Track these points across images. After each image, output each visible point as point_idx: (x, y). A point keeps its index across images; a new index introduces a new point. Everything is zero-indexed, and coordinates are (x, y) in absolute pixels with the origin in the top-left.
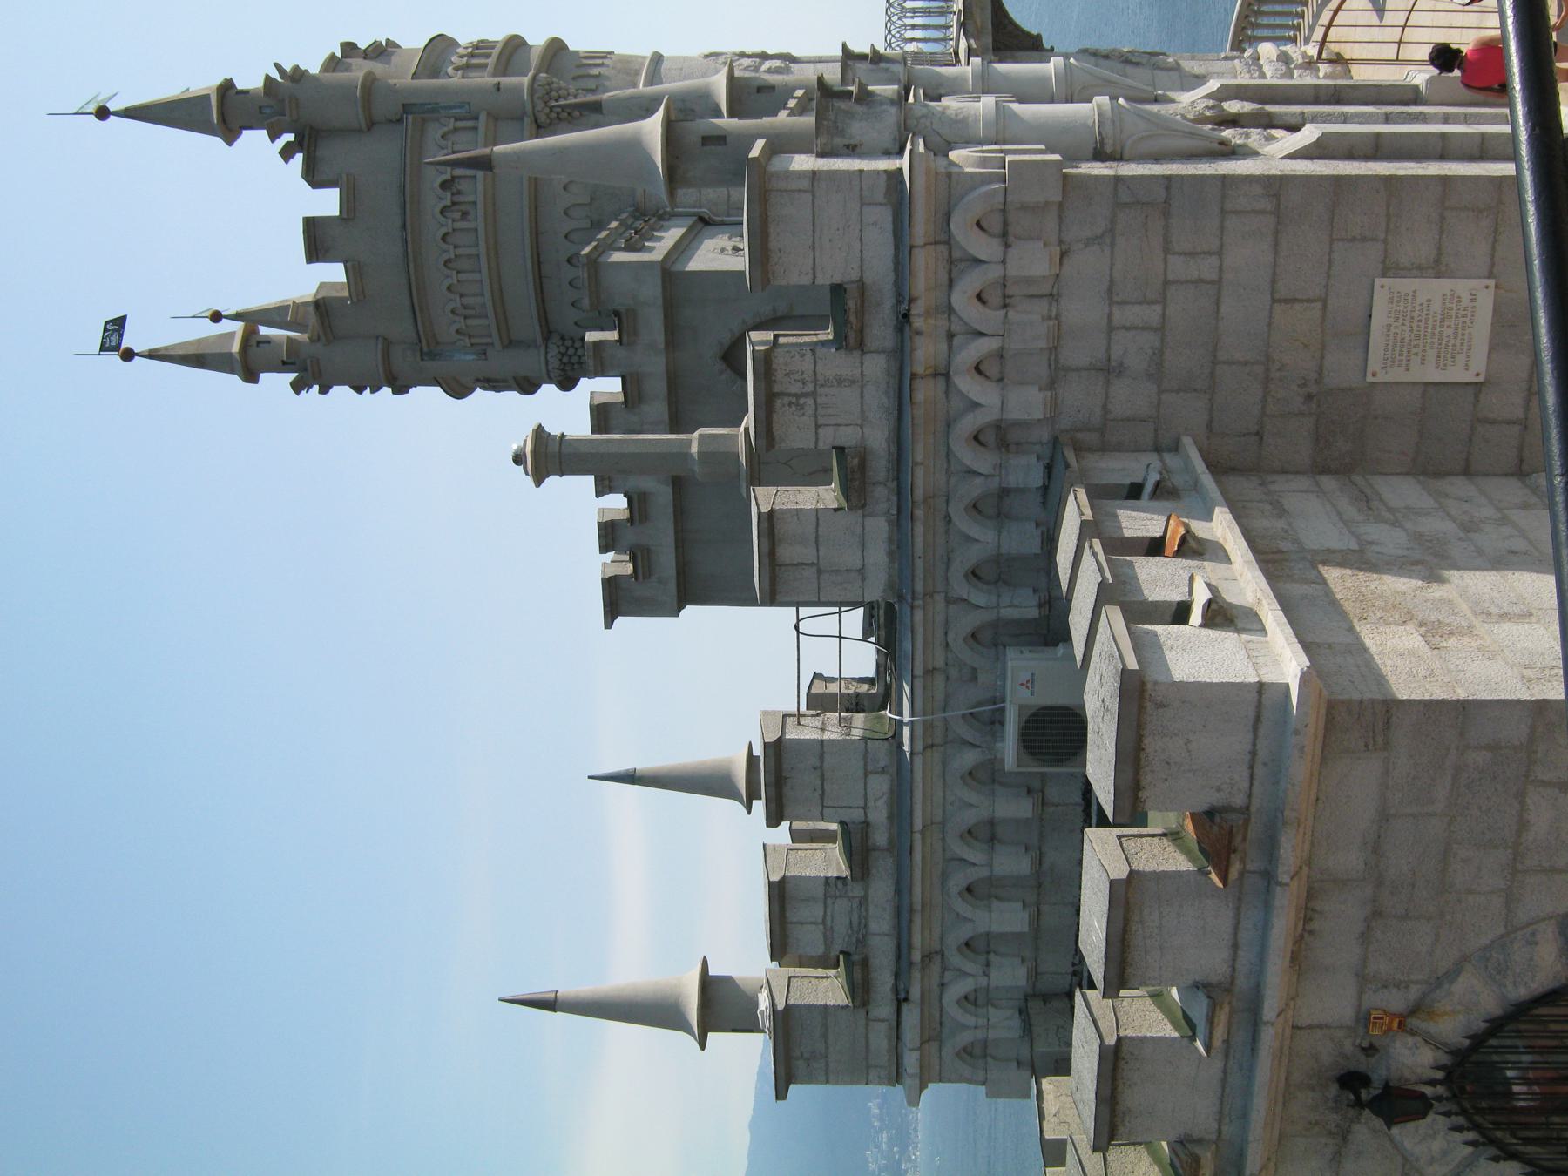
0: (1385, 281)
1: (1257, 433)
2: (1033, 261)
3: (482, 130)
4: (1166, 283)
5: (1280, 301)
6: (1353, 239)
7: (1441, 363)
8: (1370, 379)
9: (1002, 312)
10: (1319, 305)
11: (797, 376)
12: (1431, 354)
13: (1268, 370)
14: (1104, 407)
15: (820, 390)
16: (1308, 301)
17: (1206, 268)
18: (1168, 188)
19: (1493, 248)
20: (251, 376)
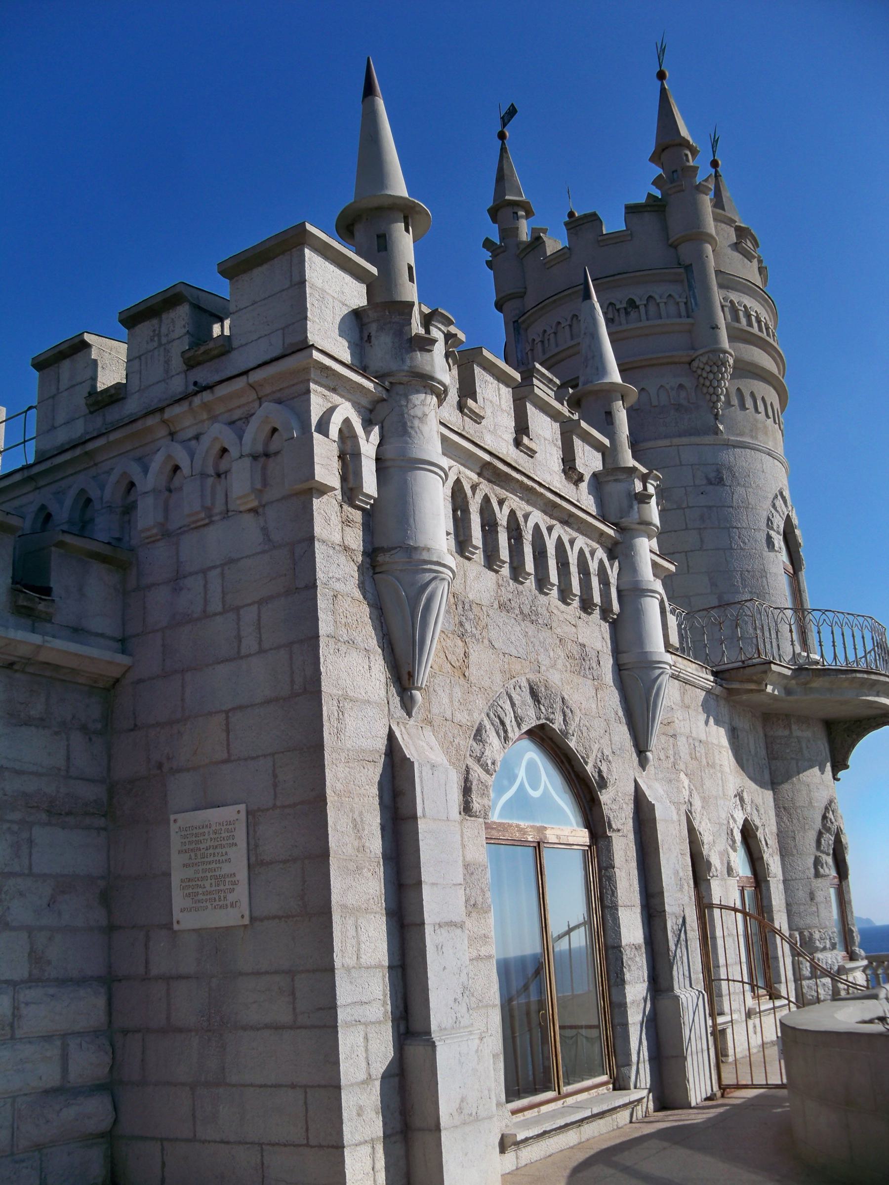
1: (136, 725)
2: (241, 481)
3: (678, 320)
4: (237, 609)
5: (227, 718)
6: (275, 776)
8: (172, 817)
9: (211, 471)
10: (225, 756)
11: (172, 328)
12: (190, 873)
14: (153, 585)
15: (162, 349)
16: (228, 745)
17: (250, 643)
18: (307, 587)
19: (274, 917)
20: (494, 213)
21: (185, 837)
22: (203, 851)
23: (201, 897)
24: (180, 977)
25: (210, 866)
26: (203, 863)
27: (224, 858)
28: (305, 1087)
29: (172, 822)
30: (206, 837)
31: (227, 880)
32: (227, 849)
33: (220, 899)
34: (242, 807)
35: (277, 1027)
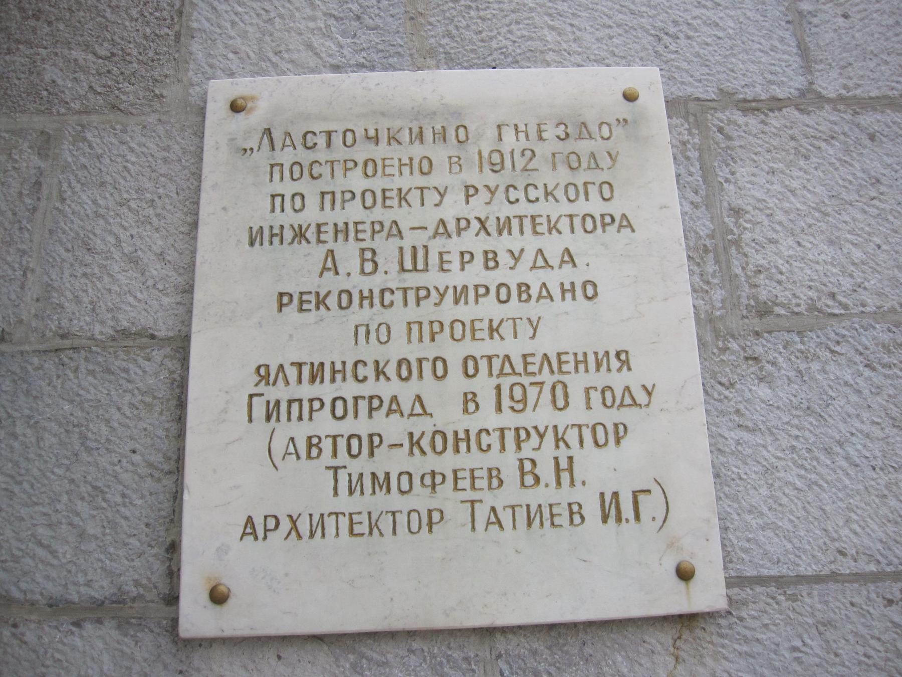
8: (221, 91)
12: (327, 337)
22: (410, 239)
23: (392, 462)
25: (465, 312)
26: (421, 295)
27: (554, 279)
29: (216, 109)
30: (437, 179)
31: (577, 384)
32: (579, 243)
33: (528, 473)
34: (648, 80)
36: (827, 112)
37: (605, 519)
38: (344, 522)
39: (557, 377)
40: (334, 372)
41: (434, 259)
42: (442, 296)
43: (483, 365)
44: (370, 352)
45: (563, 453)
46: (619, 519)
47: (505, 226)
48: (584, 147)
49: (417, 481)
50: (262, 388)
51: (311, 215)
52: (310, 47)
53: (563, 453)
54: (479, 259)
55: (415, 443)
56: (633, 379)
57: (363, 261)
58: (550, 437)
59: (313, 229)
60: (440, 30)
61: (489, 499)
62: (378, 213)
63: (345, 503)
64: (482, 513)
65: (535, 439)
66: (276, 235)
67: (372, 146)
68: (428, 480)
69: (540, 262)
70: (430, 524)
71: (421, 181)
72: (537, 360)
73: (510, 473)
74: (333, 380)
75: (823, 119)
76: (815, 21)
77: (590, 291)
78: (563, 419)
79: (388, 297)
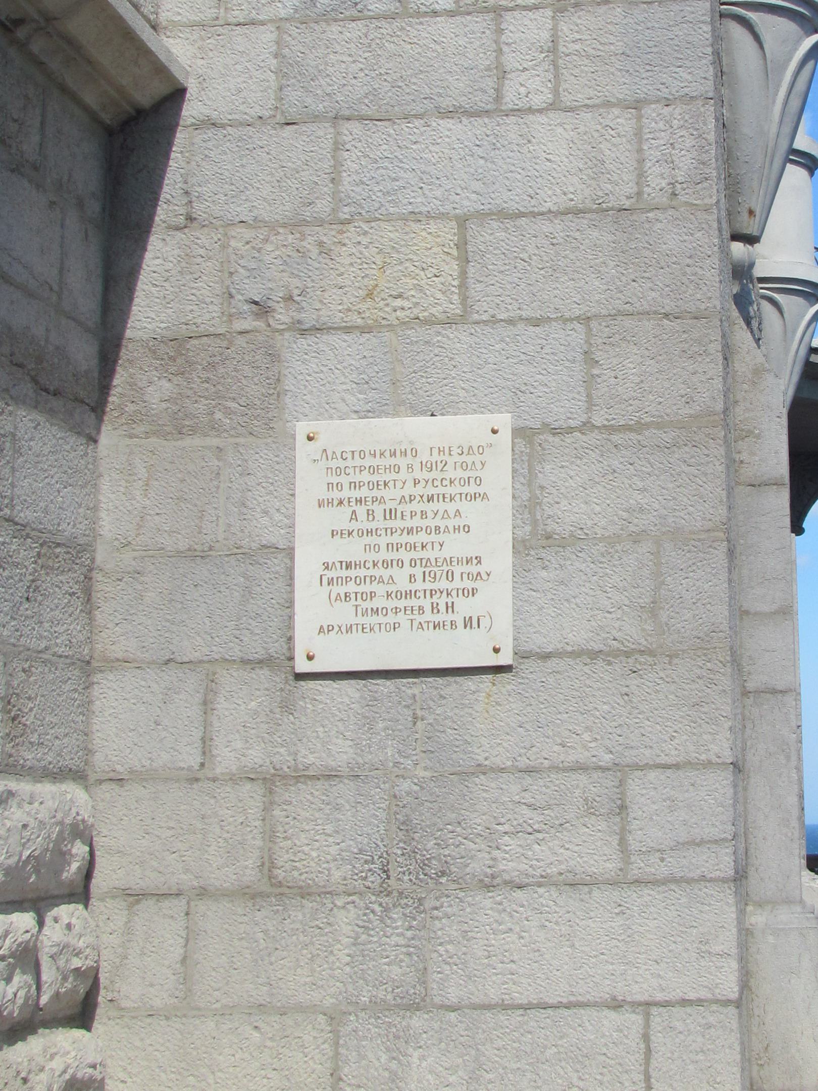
0: (506, 435)
4: (498, 11)
7: (333, 574)
8: (302, 428)
13: (321, 223)
16: (463, 286)
17: (529, 85)
21: (339, 471)
24: (301, 776)
25: (412, 539)
28: (647, 1006)
29: (301, 438)
30: (403, 475)
31: (458, 570)
32: (464, 506)
33: (435, 608)
34: (504, 421)
35: (575, 883)
36: (595, 434)
37: (465, 627)
38: (360, 627)
39: (450, 567)
40: (356, 565)
41: (399, 515)
42: (403, 531)
43: (418, 562)
44: (371, 556)
45: (450, 600)
46: (471, 627)
47: (430, 499)
48: (469, 459)
49: (389, 611)
50: (326, 572)
51: (346, 493)
52: (343, 400)
53: (450, 600)
54: (419, 514)
55: (389, 595)
56: (482, 569)
57: (368, 514)
58: (445, 593)
59: (346, 500)
60: (408, 389)
61: (419, 618)
62: (375, 493)
63: (361, 620)
64: (416, 624)
65: (438, 593)
66: (330, 502)
67: (372, 458)
68: (394, 610)
69: (446, 516)
70: (394, 628)
71: (394, 476)
72: (441, 560)
73: (428, 608)
74: (355, 568)
75: (593, 438)
76: (599, 380)
77: (466, 529)
78: (450, 586)
79: (379, 532)
